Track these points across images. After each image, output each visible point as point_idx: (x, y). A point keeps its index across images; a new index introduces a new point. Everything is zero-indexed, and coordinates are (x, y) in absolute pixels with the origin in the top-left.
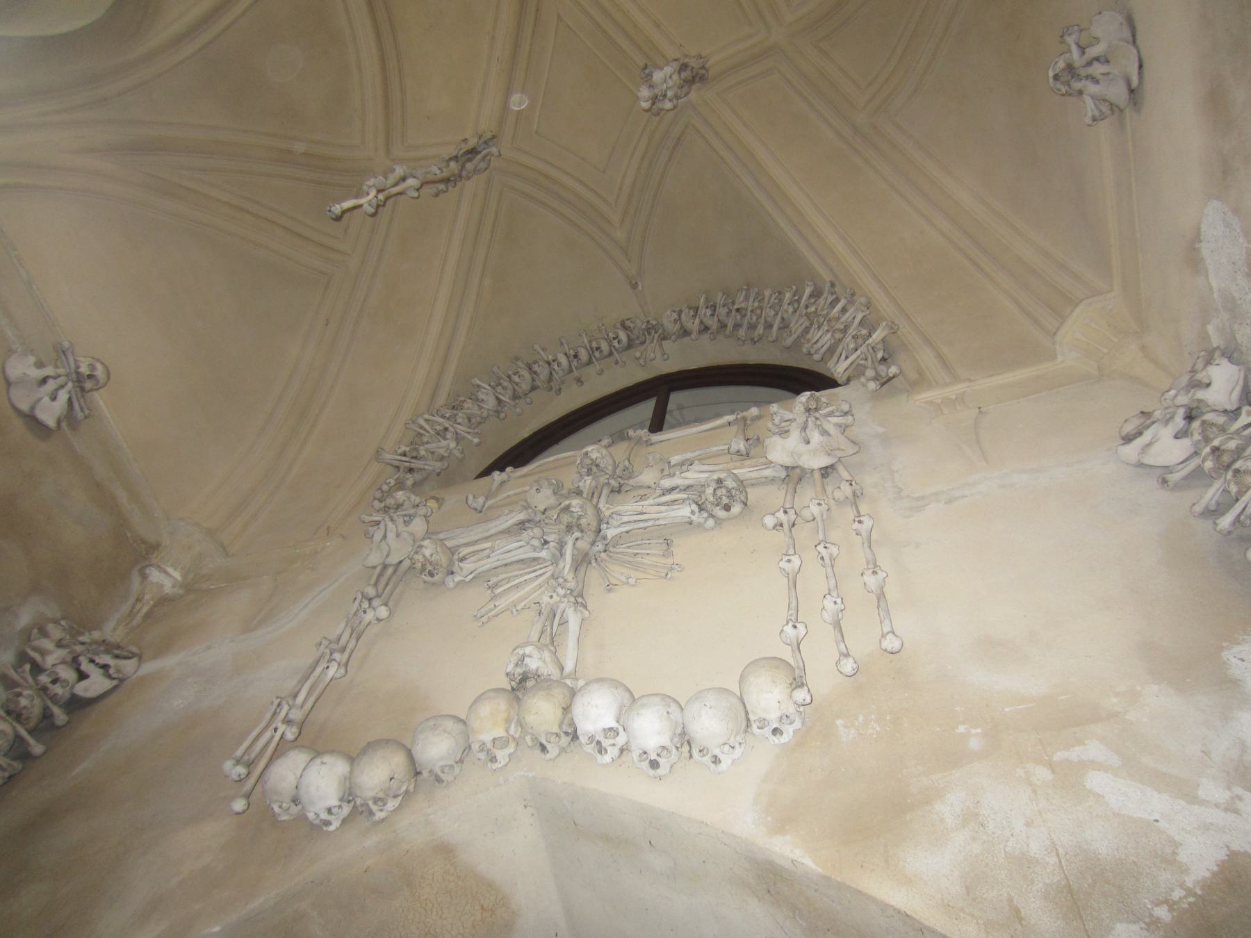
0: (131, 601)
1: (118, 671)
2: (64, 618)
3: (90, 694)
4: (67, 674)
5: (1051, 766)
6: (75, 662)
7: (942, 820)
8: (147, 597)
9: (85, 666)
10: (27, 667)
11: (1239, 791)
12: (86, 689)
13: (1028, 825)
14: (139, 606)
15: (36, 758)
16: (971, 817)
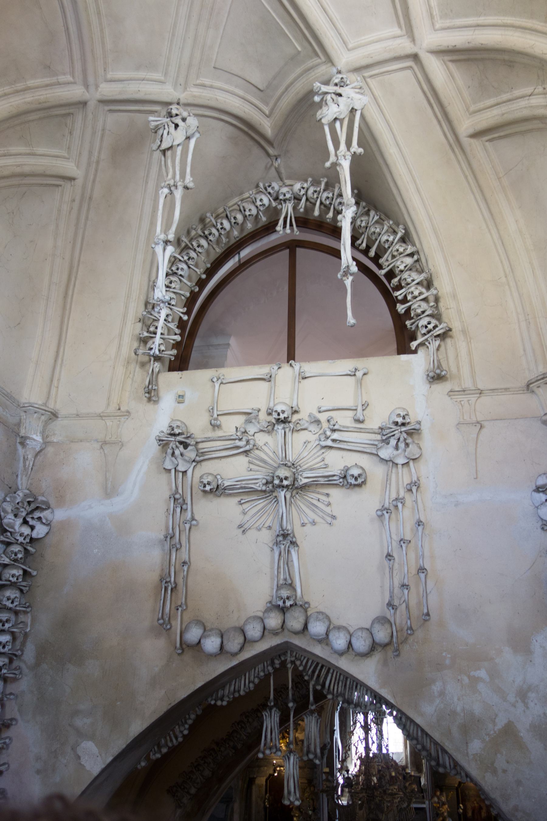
0: (22, 458)
1: (47, 520)
2: (6, 496)
3: (40, 536)
4: (26, 530)
5: (469, 677)
6: (25, 522)
7: (434, 693)
8: (29, 457)
9: (31, 522)
10: (9, 534)
11: (518, 699)
12: (38, 534)
13: (458, 699)
14: (27, 463)
15: (34, 576)
16: (442, 693)
